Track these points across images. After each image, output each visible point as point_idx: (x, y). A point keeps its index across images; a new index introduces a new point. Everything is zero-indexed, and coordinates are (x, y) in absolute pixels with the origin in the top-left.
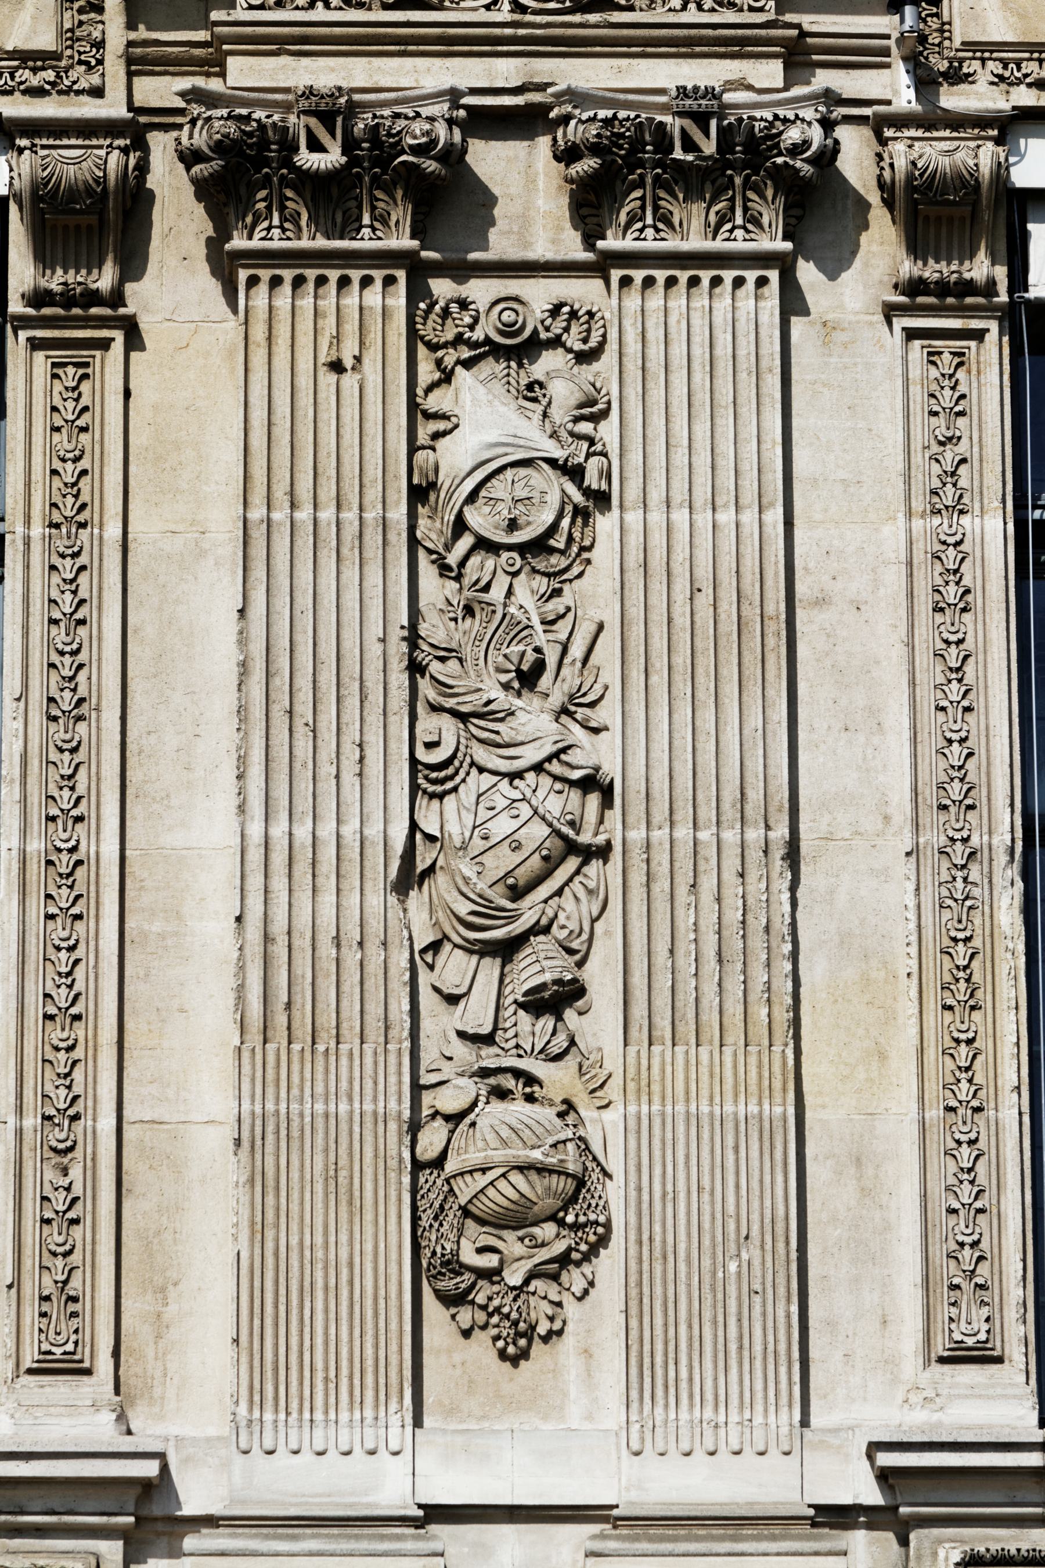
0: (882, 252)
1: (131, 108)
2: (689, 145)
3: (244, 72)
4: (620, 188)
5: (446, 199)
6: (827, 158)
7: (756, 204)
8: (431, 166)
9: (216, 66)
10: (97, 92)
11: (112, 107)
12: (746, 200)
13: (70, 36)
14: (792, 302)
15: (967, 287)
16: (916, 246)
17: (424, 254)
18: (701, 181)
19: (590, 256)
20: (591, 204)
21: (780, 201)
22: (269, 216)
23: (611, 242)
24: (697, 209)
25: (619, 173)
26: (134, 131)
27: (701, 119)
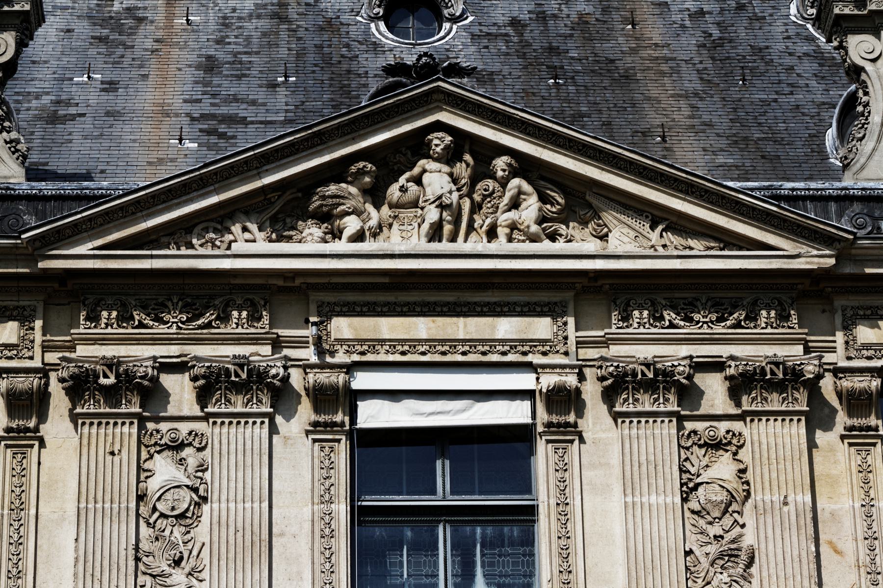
0: (305, 412)
1: (43, 363)
2: (237, 375)
3: (82, 350)
4: (213, 390)
5: (152, 394)
6: (286, 379)
7: (261, 396)
8: (146, 383)
9: (72, 349)
10: (31, 358)
11: (37, 363)
12: (257, 394)
13: (23, 339)
14: (273, 430)
15: (335, 424)
16: (317, 410)
18: (241, 388)
19: (203, 414)
21: (269, 394)
22: (90, 401)
23: (210, 409)
24: (240, 397)
25: (212, 385)
26: (44, 372)
27: (241, 366)
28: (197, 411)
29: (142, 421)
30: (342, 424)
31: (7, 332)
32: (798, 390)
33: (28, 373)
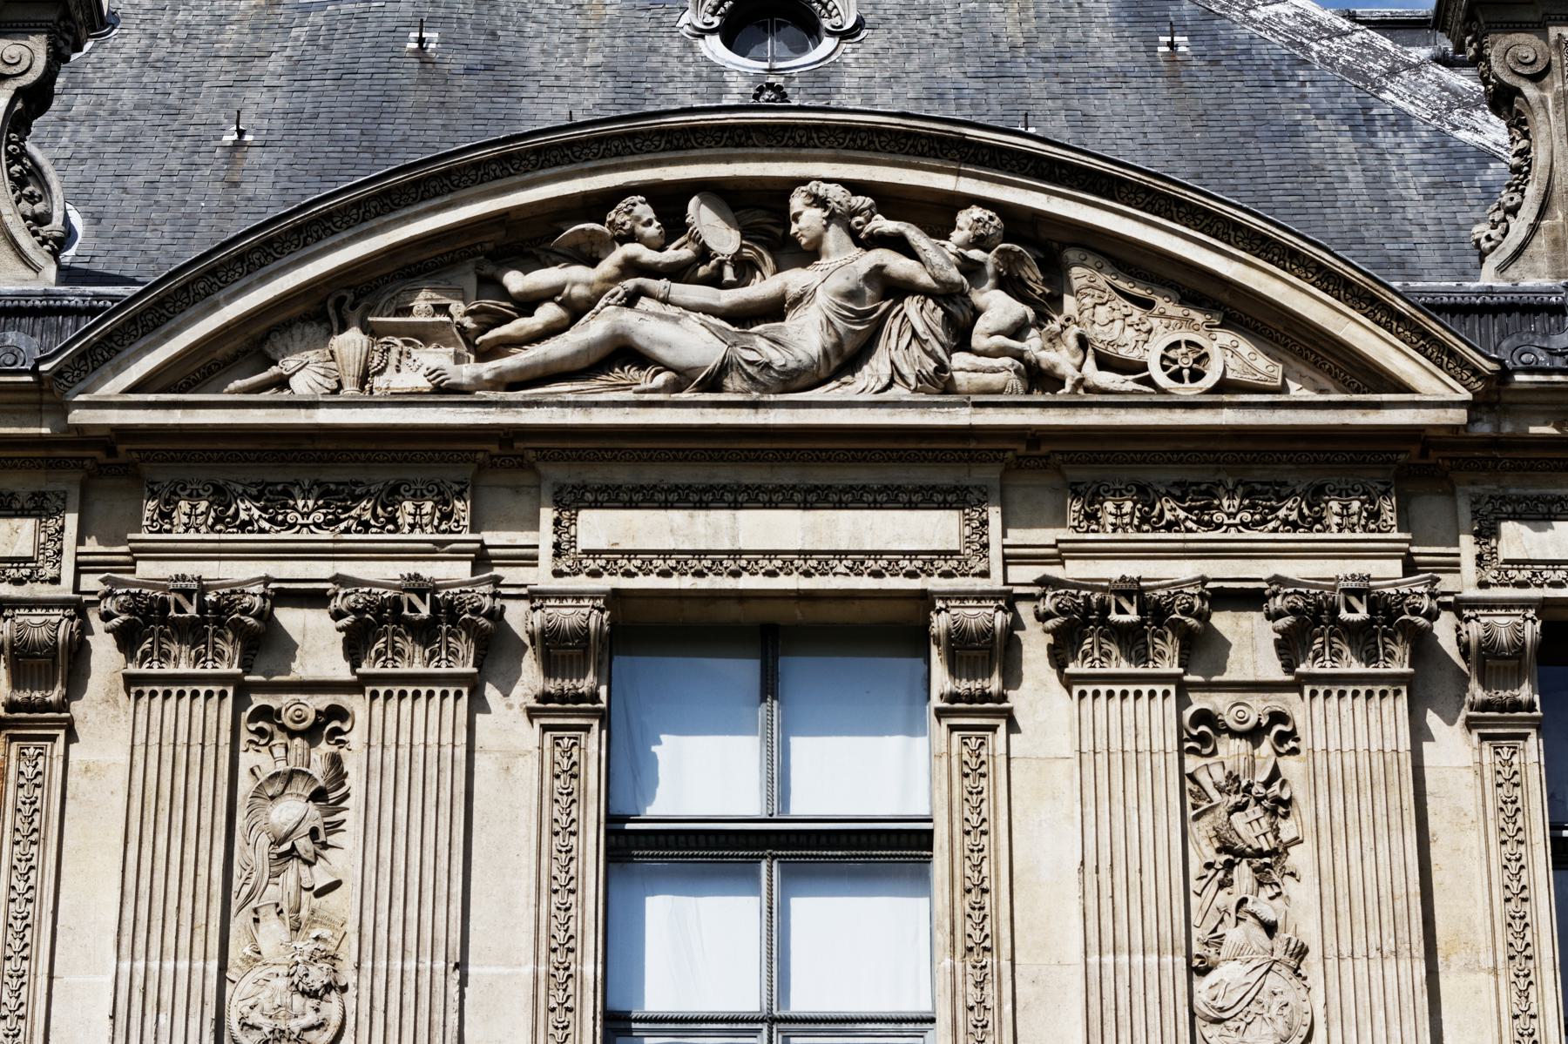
3: (147, 570)
5: (263, 642)
7: (221, 645)
11: (64, 590)
14: (478, 704)
15: (580, 698)
16: (549, 671)
17: (247, 678)
18: (191, 632)
20: (355, 647)
23: (365, 668)
28: (343, 672)
29: (243, 691)
30: (594, 698)
31: (12, 536)
32: (456, 637)
33: (48, 608)
